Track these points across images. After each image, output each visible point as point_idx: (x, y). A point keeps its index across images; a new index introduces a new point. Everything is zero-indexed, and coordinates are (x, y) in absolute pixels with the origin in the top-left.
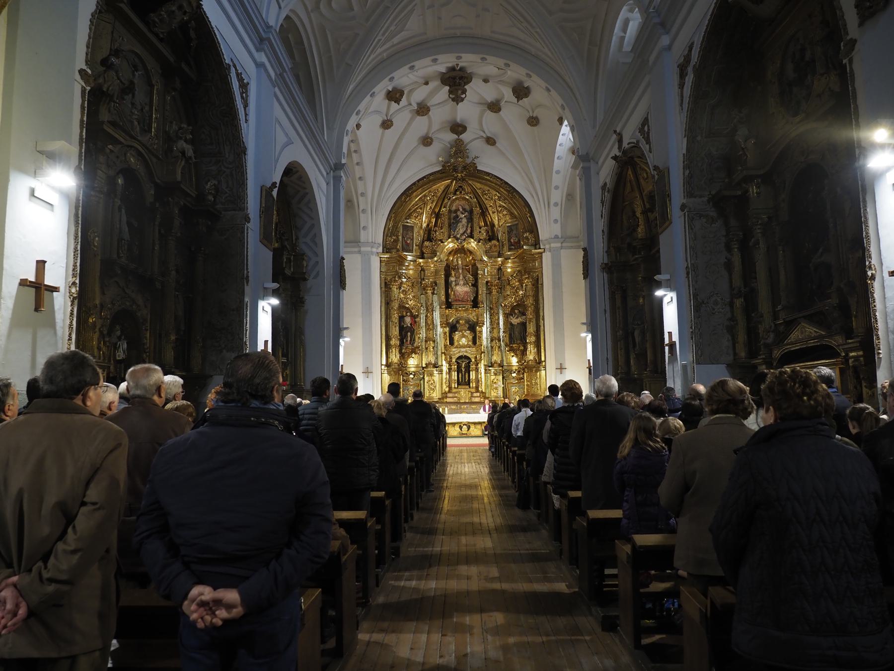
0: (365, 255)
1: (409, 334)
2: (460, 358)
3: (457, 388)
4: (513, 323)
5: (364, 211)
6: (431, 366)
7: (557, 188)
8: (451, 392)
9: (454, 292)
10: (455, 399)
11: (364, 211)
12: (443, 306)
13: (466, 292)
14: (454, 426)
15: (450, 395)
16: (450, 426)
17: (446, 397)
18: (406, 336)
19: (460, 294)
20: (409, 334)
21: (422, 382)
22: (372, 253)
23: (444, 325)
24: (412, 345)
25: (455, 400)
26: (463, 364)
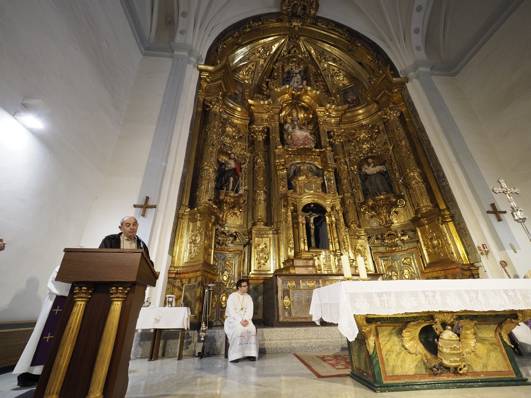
0: (178, 59)
1: (232, 179)
2: (307, 208)
3: (309, 251)
4: (368, 173)
5: (184, 15)
6: (262, 223)
7: (419, 9)
8: (300, 258)
9: (291, 137)
10: (311, 268)
11: (184, 15)
12: (279, 145)
13: (306, 136)
14: (399, 333)
15: (297, 262)
16: (385, 331)
17: (294, 267)
18: (228, 181)
19: (299, 139)
20: (232, 179)
21: (246, 249)
22: (189, 62)
23: (281, 168)
24: (237, 192)
25: (311, 270)
26: (312, 219)
